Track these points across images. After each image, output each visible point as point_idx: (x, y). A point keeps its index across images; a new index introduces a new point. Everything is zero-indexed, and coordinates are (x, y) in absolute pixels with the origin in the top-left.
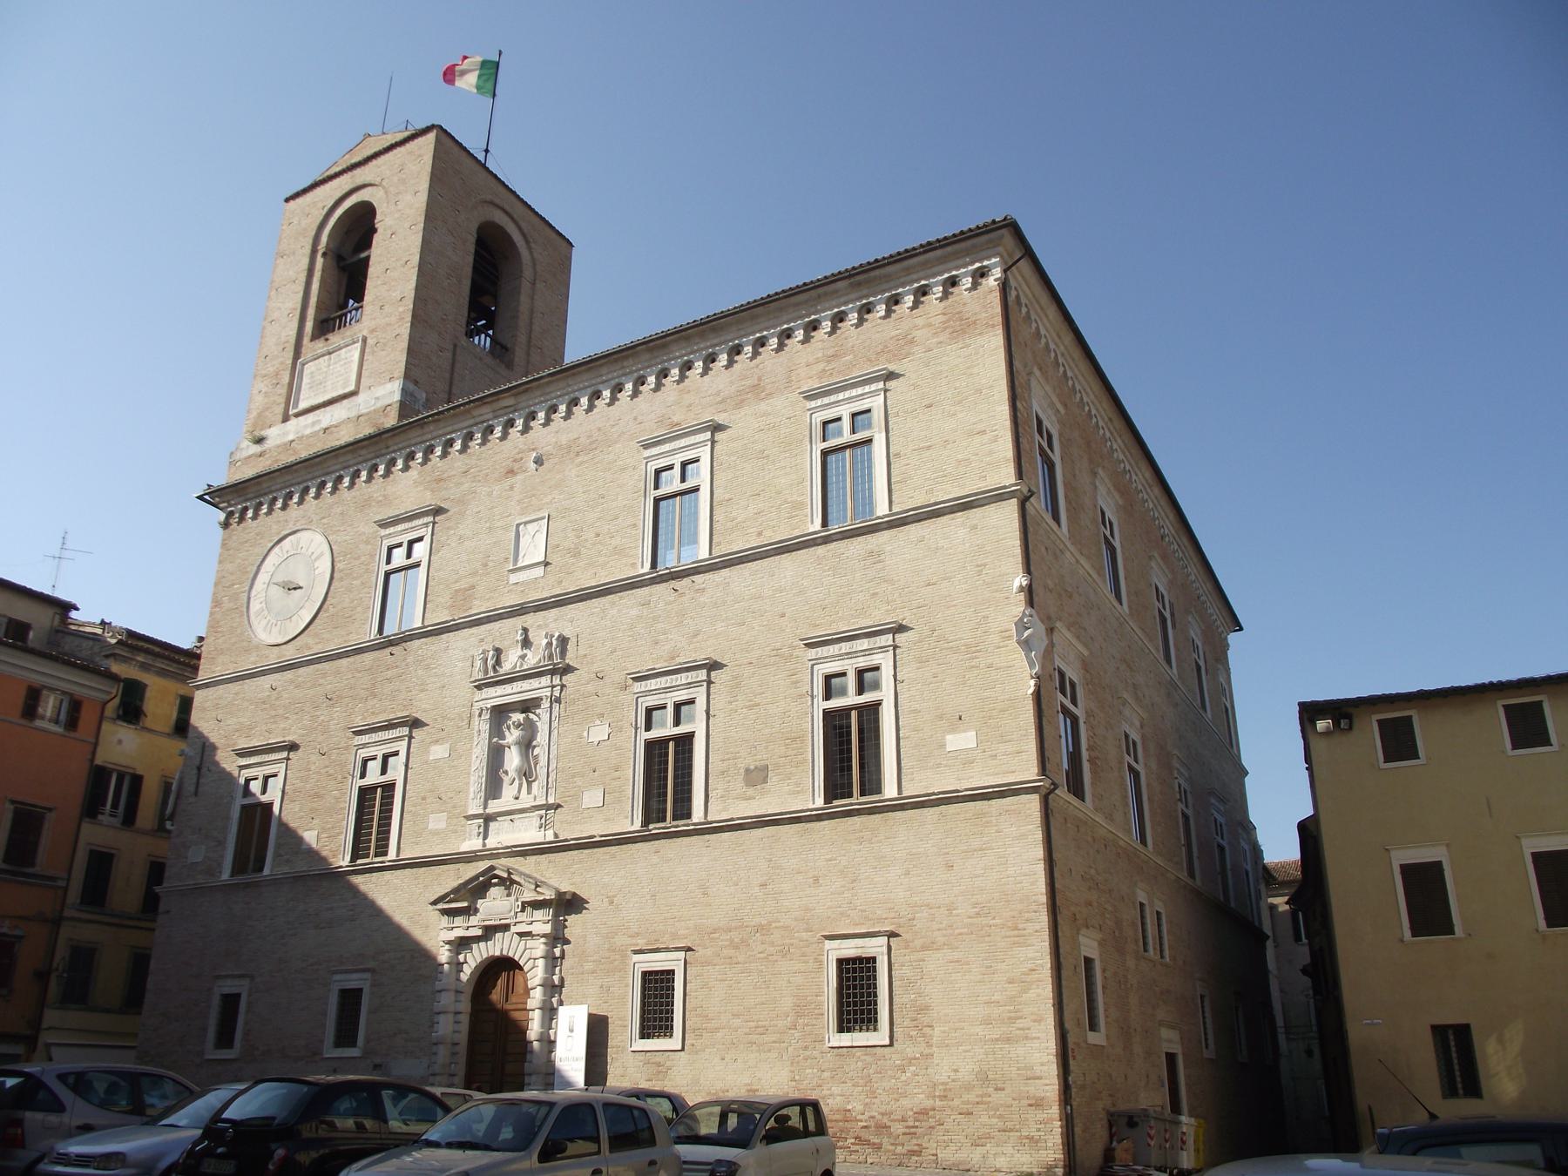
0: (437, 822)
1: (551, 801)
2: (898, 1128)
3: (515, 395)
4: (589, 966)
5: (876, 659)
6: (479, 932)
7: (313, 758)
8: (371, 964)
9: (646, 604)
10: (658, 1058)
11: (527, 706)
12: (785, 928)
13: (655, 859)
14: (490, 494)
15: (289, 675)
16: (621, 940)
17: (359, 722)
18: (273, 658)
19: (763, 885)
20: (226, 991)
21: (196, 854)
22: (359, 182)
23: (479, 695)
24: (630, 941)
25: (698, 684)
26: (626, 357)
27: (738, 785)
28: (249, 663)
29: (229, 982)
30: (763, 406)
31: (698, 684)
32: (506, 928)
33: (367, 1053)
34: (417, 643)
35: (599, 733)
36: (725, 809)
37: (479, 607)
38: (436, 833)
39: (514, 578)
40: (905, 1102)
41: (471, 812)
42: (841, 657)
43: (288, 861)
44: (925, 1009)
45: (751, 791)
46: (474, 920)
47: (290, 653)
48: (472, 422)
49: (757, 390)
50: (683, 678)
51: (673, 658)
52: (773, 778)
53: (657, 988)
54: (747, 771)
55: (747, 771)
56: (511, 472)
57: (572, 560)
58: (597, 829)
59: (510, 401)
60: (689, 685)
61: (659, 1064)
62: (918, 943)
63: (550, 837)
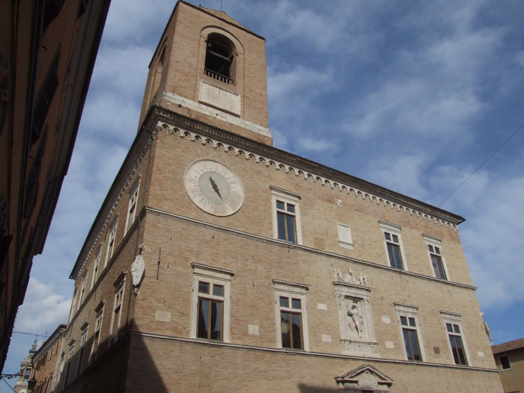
0: (326, 338)
1: (375, 342)
5: (457, 323)
7: (248, 286)
9: (392, 278)
11: (356, 299)
14: (323, 205)
15: (224, 235)
17: (274, 276)
18: (210, 220)
22: (227, 29)
23: (337, 288)
27: (433, 352)
28: (192, 215)
34: (301, 252)
35: (386, 320)
36: (431, 360)
37: (328, 250)
38: (327, 343)
39: (341, 245)
41: (343, 338)
43: (240, 338)
45: (436, 355)
47: (222, 223)
50: (410, 310)
51: (405, 301)
52: (441, 353)
56: (329, 201)
58: (392, 357)
59: (331, 175)
60: (413, 313)
63: (378, 356)
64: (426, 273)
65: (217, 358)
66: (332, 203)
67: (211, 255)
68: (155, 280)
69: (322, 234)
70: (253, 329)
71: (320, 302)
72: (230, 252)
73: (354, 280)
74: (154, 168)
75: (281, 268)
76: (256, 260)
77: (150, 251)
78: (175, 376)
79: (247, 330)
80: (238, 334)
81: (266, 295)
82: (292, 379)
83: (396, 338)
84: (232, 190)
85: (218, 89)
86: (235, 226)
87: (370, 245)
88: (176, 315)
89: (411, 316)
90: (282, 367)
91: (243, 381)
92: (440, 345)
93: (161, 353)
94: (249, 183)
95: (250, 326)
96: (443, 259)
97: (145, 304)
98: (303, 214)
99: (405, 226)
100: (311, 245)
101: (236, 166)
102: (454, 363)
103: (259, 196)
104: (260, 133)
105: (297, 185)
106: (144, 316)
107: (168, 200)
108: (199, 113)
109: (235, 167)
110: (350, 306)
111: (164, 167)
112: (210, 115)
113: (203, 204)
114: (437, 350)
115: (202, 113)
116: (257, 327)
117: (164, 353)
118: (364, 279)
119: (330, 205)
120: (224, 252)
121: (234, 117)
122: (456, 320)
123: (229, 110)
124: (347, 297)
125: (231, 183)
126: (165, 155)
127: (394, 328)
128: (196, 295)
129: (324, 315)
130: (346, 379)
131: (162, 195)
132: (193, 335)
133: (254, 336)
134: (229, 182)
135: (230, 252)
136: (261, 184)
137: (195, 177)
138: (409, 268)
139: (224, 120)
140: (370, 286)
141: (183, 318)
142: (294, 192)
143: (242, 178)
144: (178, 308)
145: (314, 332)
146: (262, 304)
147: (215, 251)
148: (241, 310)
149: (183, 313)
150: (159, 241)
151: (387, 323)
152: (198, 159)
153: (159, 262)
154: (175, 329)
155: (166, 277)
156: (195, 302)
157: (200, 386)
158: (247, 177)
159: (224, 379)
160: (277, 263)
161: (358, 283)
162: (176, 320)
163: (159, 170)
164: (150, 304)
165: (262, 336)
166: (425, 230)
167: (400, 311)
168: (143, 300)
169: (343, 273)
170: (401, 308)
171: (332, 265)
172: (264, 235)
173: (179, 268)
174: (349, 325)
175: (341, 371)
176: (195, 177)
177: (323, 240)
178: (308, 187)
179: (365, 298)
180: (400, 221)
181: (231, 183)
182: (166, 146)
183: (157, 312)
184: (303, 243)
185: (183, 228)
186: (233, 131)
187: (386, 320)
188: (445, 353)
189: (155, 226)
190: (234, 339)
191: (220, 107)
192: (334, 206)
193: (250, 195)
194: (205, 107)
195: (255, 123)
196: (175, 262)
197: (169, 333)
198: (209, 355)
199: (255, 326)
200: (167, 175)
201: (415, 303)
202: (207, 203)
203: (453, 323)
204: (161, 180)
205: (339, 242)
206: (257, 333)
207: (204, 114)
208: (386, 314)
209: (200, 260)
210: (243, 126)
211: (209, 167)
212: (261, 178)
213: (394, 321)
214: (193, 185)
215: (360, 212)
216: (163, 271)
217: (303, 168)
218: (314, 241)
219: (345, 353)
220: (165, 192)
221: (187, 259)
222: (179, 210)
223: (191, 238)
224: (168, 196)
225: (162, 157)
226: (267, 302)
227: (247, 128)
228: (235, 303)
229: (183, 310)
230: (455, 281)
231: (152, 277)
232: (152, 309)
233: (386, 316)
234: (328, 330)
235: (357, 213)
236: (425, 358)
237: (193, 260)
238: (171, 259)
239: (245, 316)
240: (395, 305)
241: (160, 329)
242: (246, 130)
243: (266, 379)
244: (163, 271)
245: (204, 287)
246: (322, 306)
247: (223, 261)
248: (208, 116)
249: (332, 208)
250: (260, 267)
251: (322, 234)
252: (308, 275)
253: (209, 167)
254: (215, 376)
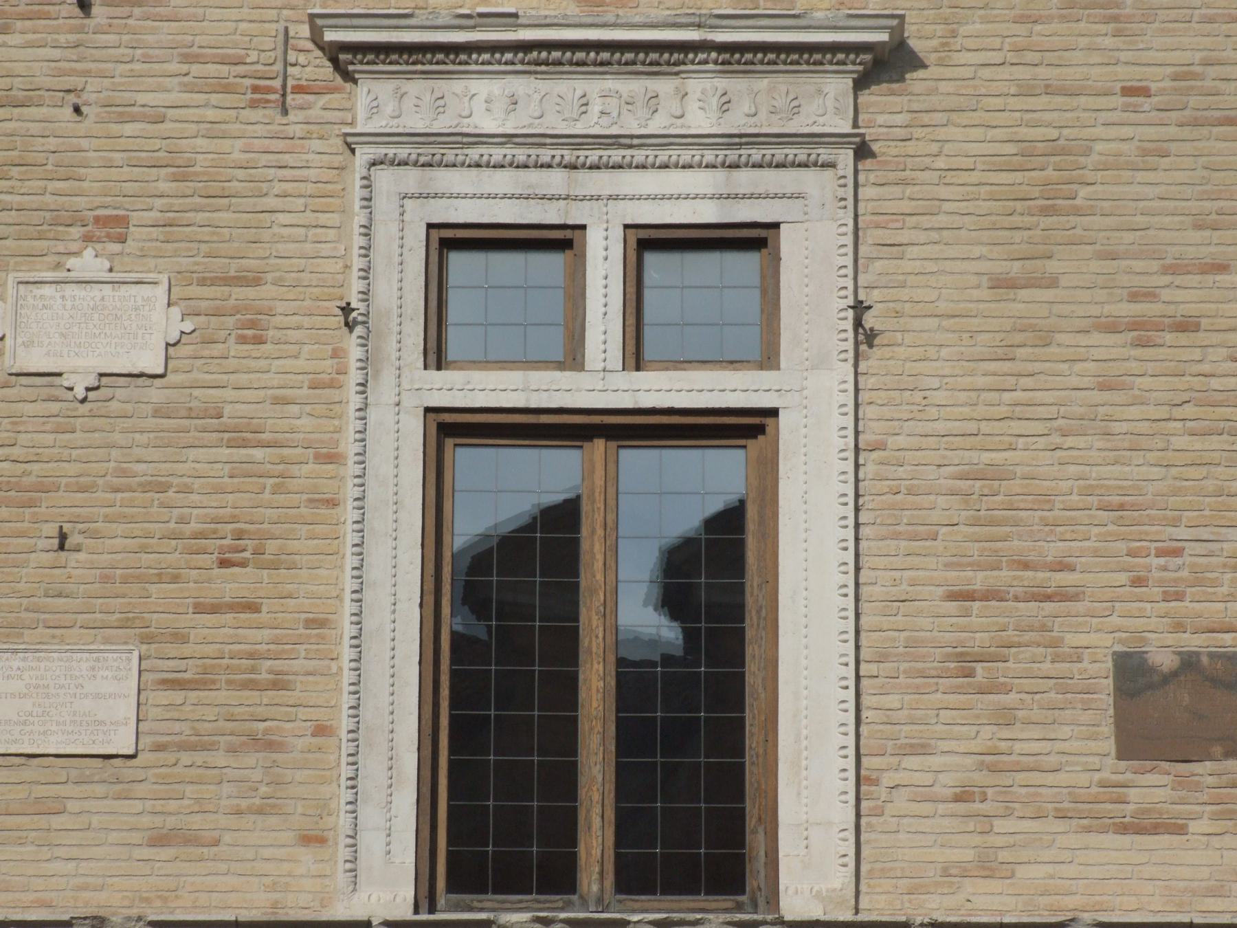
25: (804, 150)
27: (1084, 741)
31: (804, 150)
36: (987, 868)
45: (1154, 787)
50: (698, 103)
54: (1132, 674)
55: (1132, 674)
60: (737, 149)
83: (233, 583)
89: (690, 198)
127: (242, 435)
151: (80, 366)
170: (485, 102)
208: (110, 228)
213: (253, 332)
233: (89, 263)
240: (346, 60)
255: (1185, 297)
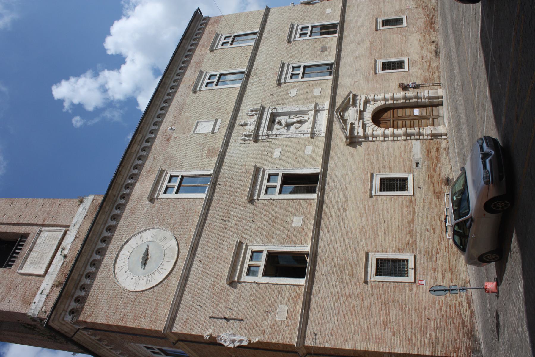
0: (309, 151)
2: (428, 13)
3: (140, 133)
4: (379, 86)
5: (300, 28)
6: (361, 121)
7: (253, 227)
8: (369, 175)
10: (411, 63)
12: (372, 38)
13: (344, 71)
14: (172, 146)
16: (371, 77)
17: (245, 199)
18: (181, 264)
19: (358, 44)
20: (374, 272)
21: (281, 313)
24: (371, 75)
26: (158, 94)
27: (325, 53)
28: (175, 282)
29: (369, 269)
30: (205, 61)
32: (360, 111)
33: (410, 170)
37: (220, 144)
38: (314, 151)
39: (216, 131)
40: (421, 12)
42: (296, 34)
43: (305, 236)
44: (397, 11)
45: (328, 50)
46: (356, 125)
47: (185, 251)
48: (135, 155)
49: (198, 64)
51: (276, 73)
53: (386, 66)
57: (222, 110)
61: (413, 63)
62: (380, 14)
64: (249, 52)
65: (325, 258)
66: (171, 137)
67: (220, 263)
68: (243, 324)
69: (203, 148)
70: (297, 221)
71: (272, 155)
72: (216, 244)
73: (252, 120)
74: (120, 324)
75: (236, 192)
76: (226, 218)
77: (212, 328)
78: (342, 299)
79: (298, 228)
80: (301, 237)
81: (263, 208)
82: (347, 186)
84: (149, 240)
85: (32, 253)
86: (190, 238)
87: (217, 102)
88: (281, 300)
89: (290, 69)
90: (335, 195)
91: (348, 232)
92: (319, 46)
93: (319, 314)
94: (143, 220)
95: (293, 225)
96: (236, 34)
97: (268, 331)
98: (181, 167)
99: (200, 66)
100: (214, 161)
101: (123, 234)
102: (337, 35)
103: (158, 212)
104: (87, 208)
105: (149, 171)
106: (281, 333)
107: (157, 309)
108: (58, 274)
109: (124, 236)
110: (279, 127)
111: (118, 314)
112: (62, 262)
113: (163, 270)
114: (324, 49)
115: (60, 271)
116: (295, 218)
117: (319, 311)
118: (252, 111)
119: (172, 139)
120: (217, 250)
121: (67, 236)
122: (297, 29)
123: (58, 241)
124: (270, 128)
125: (141, 240)
126: (105, 312)
128: (260, 278)
129: (285, 151)
130: (348, 133)
131: (151, 315)
132: (302, 281)
133: (304, 222)
134: (141, 243)
135: (216, 244)
136: (145, 210)
137: (132, 279)
138: (244, 66)
139: (69, 247)
140: (260, 105)
141: (284, 292)
142: (154, 176)
143: (136, 229)
144: (273, 297)
145: (302, 162)
146: (272, 212)
147: (216, 259)
148: (278, 233)
149: (279, 292)
150: (203, 319)
151: (296, 92)
152: (113, 275)
153: (225, 318)
154: (296, 300)
155: (241, 311)
156: (267, 280)
157: (352, 275)
158: (136, 224)
159: (345, 251)
160: (230, 196)
161: (255, 117)
162: (286, 299)
163: (122, 319)
164: (269, 327)
165: (305, 214)
166: (206, 48)
167: (285, 79)
168: (264, 333)
169: (244, 131)
171: (235, 141)
172: (200, 208)
173: (232, 298)
174: (297, 129)
175: (341, 138)
176: (132, 279)
177: (209, 149)
178: (152, 160)
179: (270, 111)
180: (195, 71)
181: (141, 240)
182: (95, 311)
183: (277, 319)
184: (211, 169)
185: (189, 292)
186: (83, 236)
187: (293, 92)
188: (327, 42)
189: (185, 322)
190: (306, 241)
191: (53, 251)
192: (174, 135)
193: (156, 221)
194: (52, 267)
195: (75, 213)
196: (226, 301)
197: (299, 306)
198: (321, 266)
199: (294, 220)
200: (129, 310)
201: (279, 65)
202: (162, 267)
203: (299, 32)
204: (134, 316)
205: (213, 133)
206: (301, 218)
207: (61, 269)
208: (287, 93)
209: (224, 274)
210: (77, 226)
211: (123, 264)
212: (139, 209)
214: (141, 281)
215: (182, 109)
216: (235, 314)
217: (130, 164)
218: (210, 158)
219: (324, 135)
220: (148, 312)
221: (222, 289)
222: (169, 297)
223: (200, 284)
224: (153, 309)
225: (107, 316)
226: (270, 207)
227: (80, 222)
228: (270, 239)
229: (276, 292)
230: (259, 25)
231: (241, 325)
232: (274, 325)
233: (289, 93)
234: (301, 148)
235: (183, 113)
236: (332, 60)
237: (224, 282)
238: (222, 306)
239: (284, 230)
241: (295, 316)
242: (82, 223)
243: (346, 210)
244: (235, 314)
245: (251, 271)
246: (277, 153)
247: (225, 251)
248: (63, 264)
249: (176, 138)
250: (235, 213)
251: (203, 148)
252: (245, 165)
253: (123, 264)
254: (342, 260)
255: (300, 51)
